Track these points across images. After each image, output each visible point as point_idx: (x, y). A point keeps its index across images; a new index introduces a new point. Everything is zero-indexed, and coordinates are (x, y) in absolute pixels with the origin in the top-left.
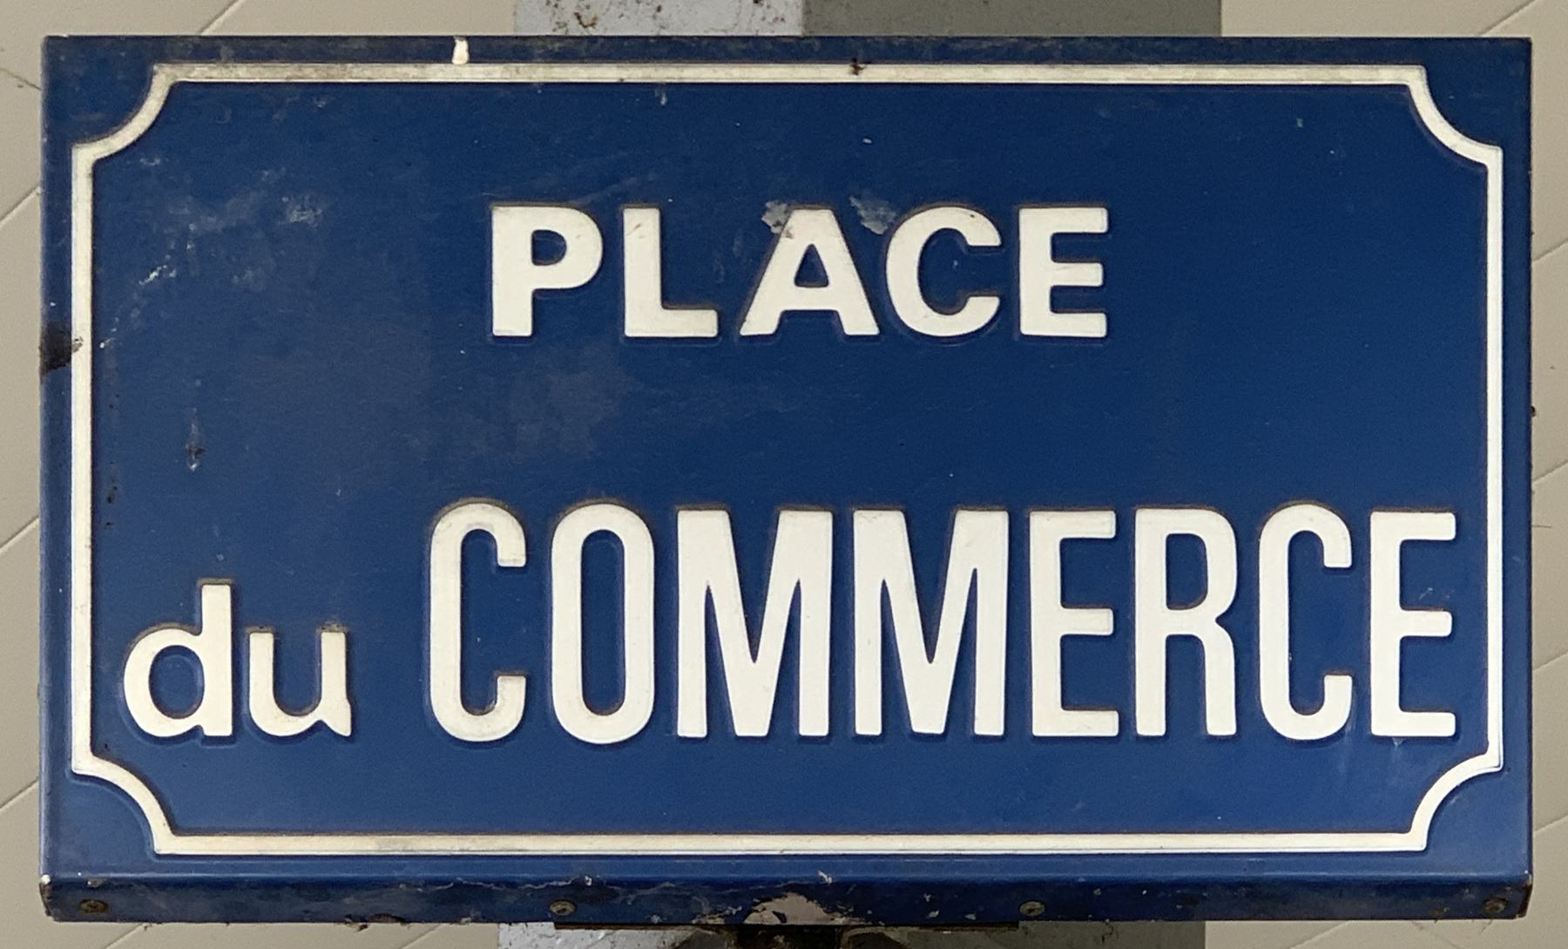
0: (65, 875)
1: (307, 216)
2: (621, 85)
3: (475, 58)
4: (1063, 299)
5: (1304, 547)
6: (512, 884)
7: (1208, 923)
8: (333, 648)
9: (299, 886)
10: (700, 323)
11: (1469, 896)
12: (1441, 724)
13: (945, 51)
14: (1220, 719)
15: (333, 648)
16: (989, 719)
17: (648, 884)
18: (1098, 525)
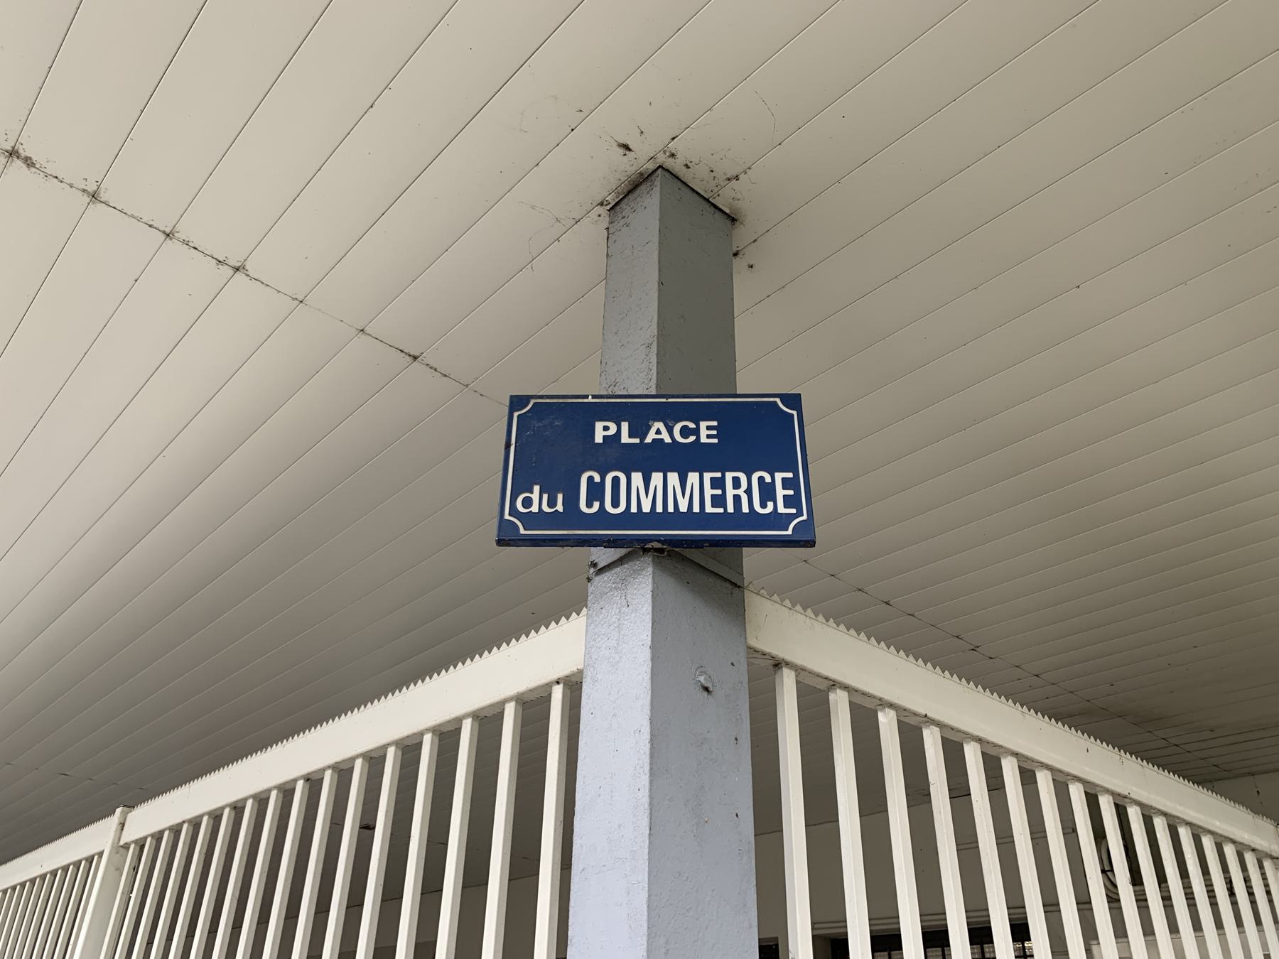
0: (501, 538)
1: (559, 424)
2: (621, 402)
3: (593, 398)
4: (709, 436)
5: (761, 479)
6: (595, 540)
7: (744, 548)
8: (560, 497)
9: (550, 540)
10: (637, 441)
11: (802, 543)
12: (794, 511)
13: (684, 397)
14: (745, 509)
15: (560, 497)
16: (696, 509)
17: (625, 540)
18: (719, 475)
